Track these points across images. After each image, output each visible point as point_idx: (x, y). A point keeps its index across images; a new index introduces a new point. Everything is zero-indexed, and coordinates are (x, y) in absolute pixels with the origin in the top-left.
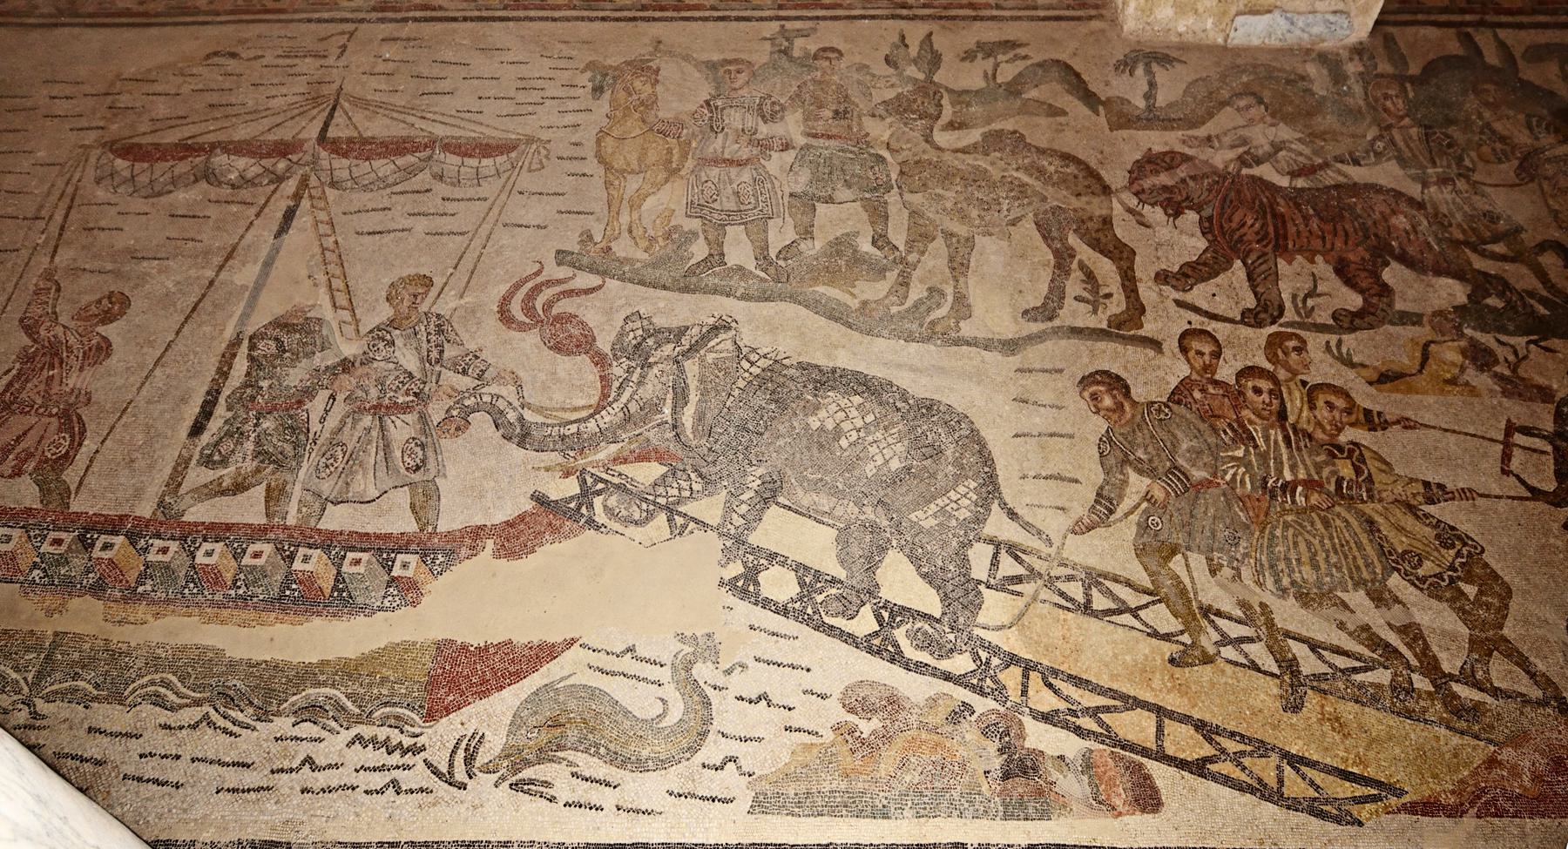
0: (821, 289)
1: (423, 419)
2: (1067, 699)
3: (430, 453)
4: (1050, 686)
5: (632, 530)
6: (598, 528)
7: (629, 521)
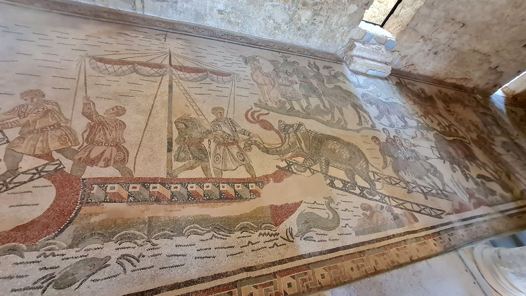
0: (318, 117)
1: (238, 146)
2: (397, 202)
3: (245, 156)
4: (393, 200)
5: (303, 173)
6: (295, 173)
7: (301, 172)
